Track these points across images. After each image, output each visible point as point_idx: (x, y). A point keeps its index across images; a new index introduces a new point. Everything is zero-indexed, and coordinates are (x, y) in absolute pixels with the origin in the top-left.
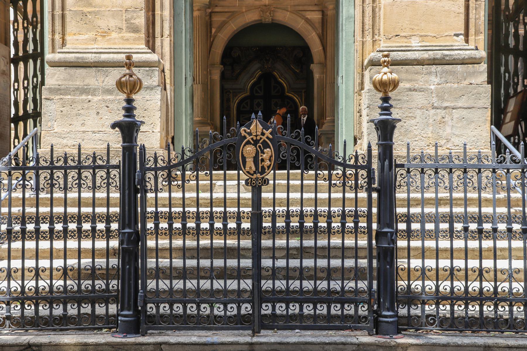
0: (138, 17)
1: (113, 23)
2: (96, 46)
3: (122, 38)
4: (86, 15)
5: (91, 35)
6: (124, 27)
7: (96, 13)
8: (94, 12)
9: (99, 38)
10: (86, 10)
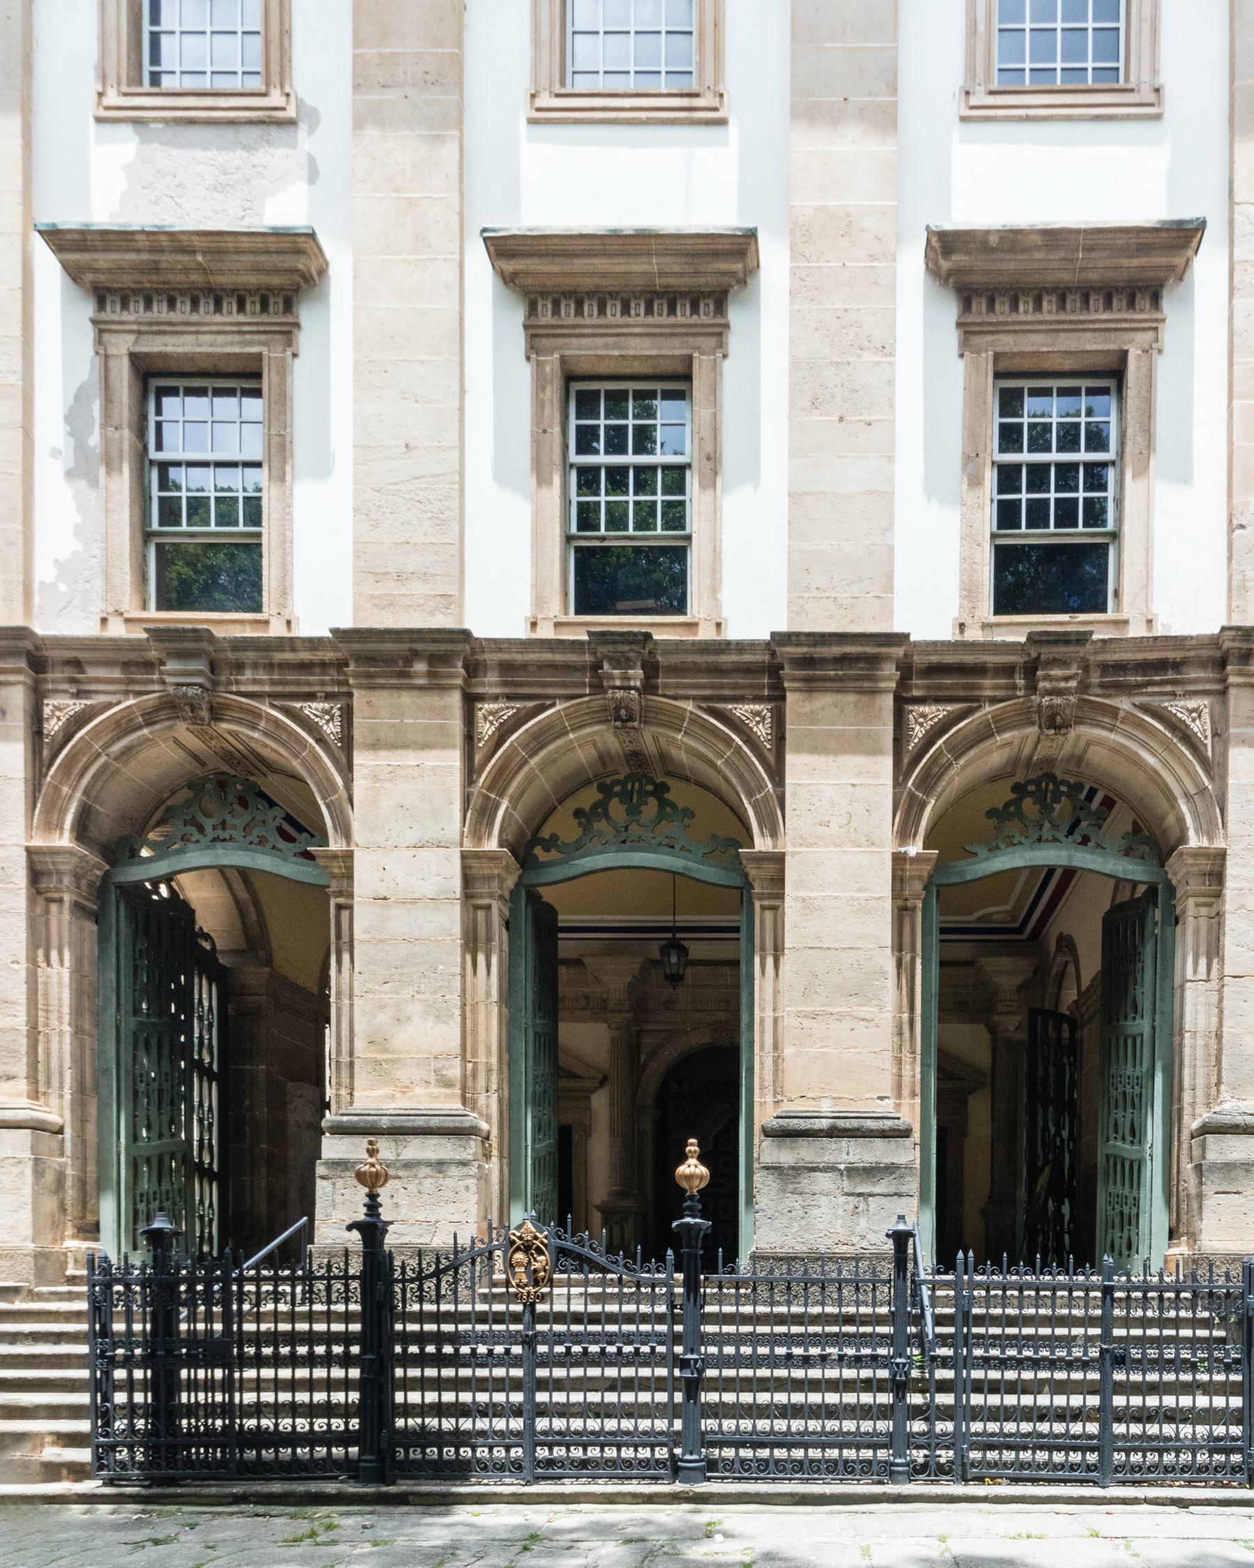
0: (452, 1067)
1: (417, 1074)
2: (393, 1106)
3: (429, 1095)
4: (377, 1063)
5: (388, 1090)
6: (433, 1078)
7: (394, 1061)
8: (391, 1060)
9: (398, 1095)
10: (380, 1057)
